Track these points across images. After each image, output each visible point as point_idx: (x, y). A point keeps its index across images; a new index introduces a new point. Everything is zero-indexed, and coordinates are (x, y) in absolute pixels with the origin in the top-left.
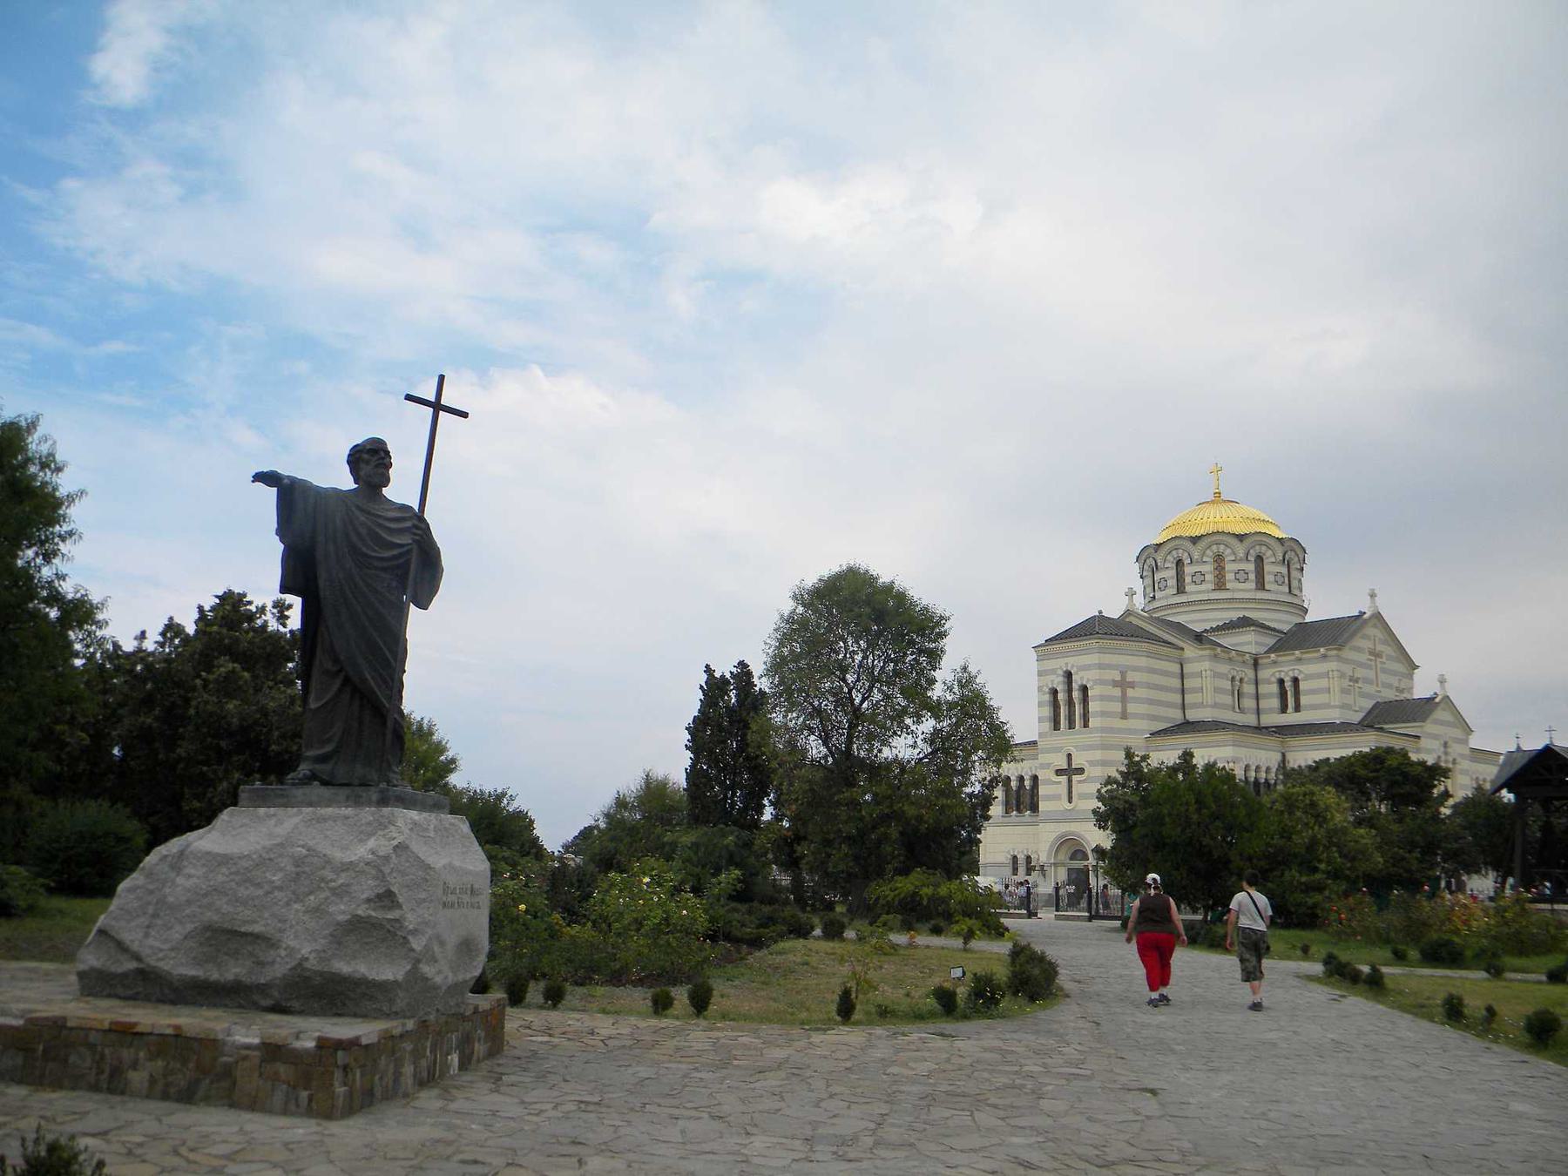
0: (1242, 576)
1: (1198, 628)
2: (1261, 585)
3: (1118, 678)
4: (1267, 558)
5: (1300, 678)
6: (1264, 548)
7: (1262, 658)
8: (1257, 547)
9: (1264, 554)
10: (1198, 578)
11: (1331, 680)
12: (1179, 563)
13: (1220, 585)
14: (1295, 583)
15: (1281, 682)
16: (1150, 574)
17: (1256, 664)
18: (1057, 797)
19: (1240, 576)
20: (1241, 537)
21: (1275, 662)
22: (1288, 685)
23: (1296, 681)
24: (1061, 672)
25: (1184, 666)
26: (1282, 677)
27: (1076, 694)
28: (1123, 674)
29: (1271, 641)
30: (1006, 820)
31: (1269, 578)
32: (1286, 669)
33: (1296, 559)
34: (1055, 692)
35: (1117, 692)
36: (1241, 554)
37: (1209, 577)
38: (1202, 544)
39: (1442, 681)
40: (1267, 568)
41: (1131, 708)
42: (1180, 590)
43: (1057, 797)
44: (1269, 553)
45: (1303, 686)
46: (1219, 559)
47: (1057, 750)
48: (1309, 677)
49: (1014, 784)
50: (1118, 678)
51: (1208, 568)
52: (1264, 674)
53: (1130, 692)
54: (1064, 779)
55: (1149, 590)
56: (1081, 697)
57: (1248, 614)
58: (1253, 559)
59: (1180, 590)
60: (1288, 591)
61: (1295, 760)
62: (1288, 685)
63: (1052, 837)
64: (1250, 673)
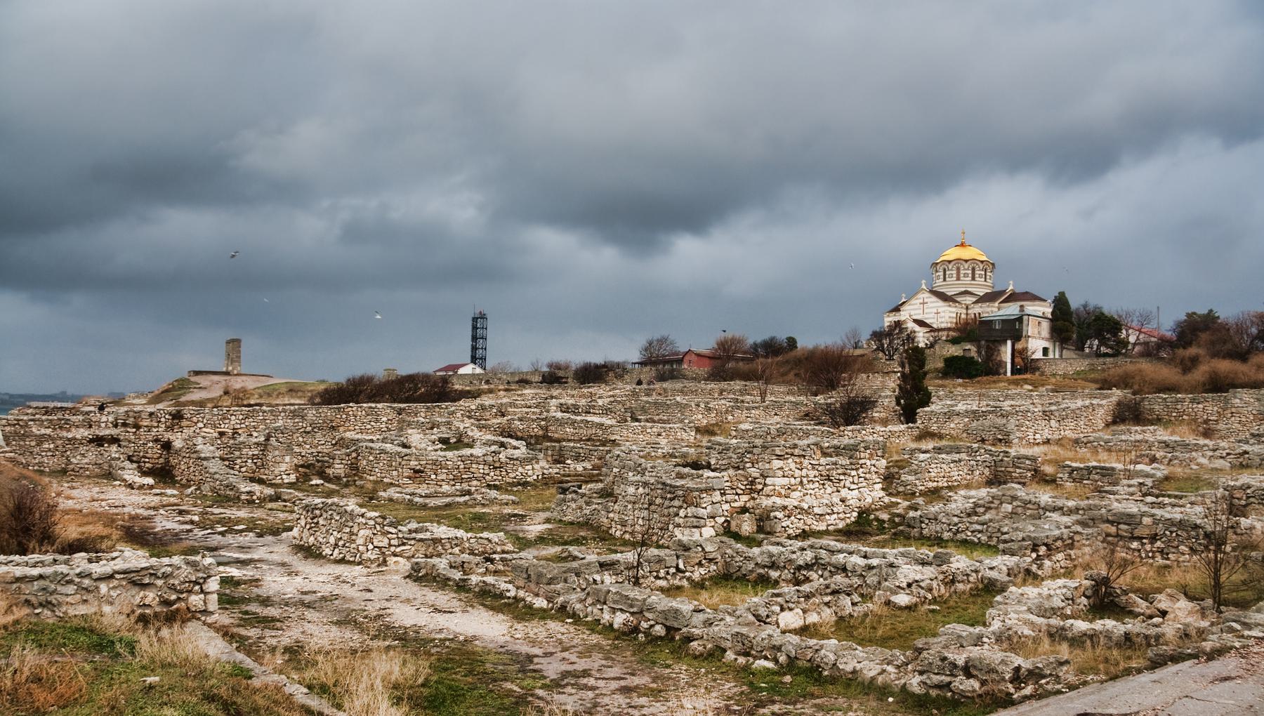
1: (949, 294)
2: (973, 279)
12: (945, 270)
13: (958, 279)
14: (988, 277)
17: (967, 308)
19: (966, 275)
20: (966, 261)
29: (974, 300)
36: (966, 267)
37: (955, 275)
38: (953, 263)
40: (977, 272)
42: (945, 280)
46: (958, 269)
51: (955, 272)
52: (969, 312)
57: (969, 289)
59: (945, 280)
60: (983, 279)
64: (965, 311)
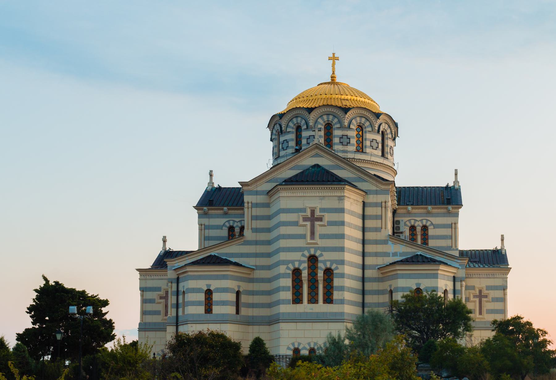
0: (375, 145)
6: (387, 126)
10: (345, 140)
11: (453, 229)
15: (413, 228)
16: (294, 130)
21: (409, 213)
22: (419, 229)
23: (425, 228)
26: (413, 224)
31: (387, 149)
32: (418, 219)
37: (353, 141)
39: (502, 240)
44: (389, 131)
45: (431, 232)
48: (436, 226)
51: (353, 134)
55: (292, 144)
62: (419, 229)
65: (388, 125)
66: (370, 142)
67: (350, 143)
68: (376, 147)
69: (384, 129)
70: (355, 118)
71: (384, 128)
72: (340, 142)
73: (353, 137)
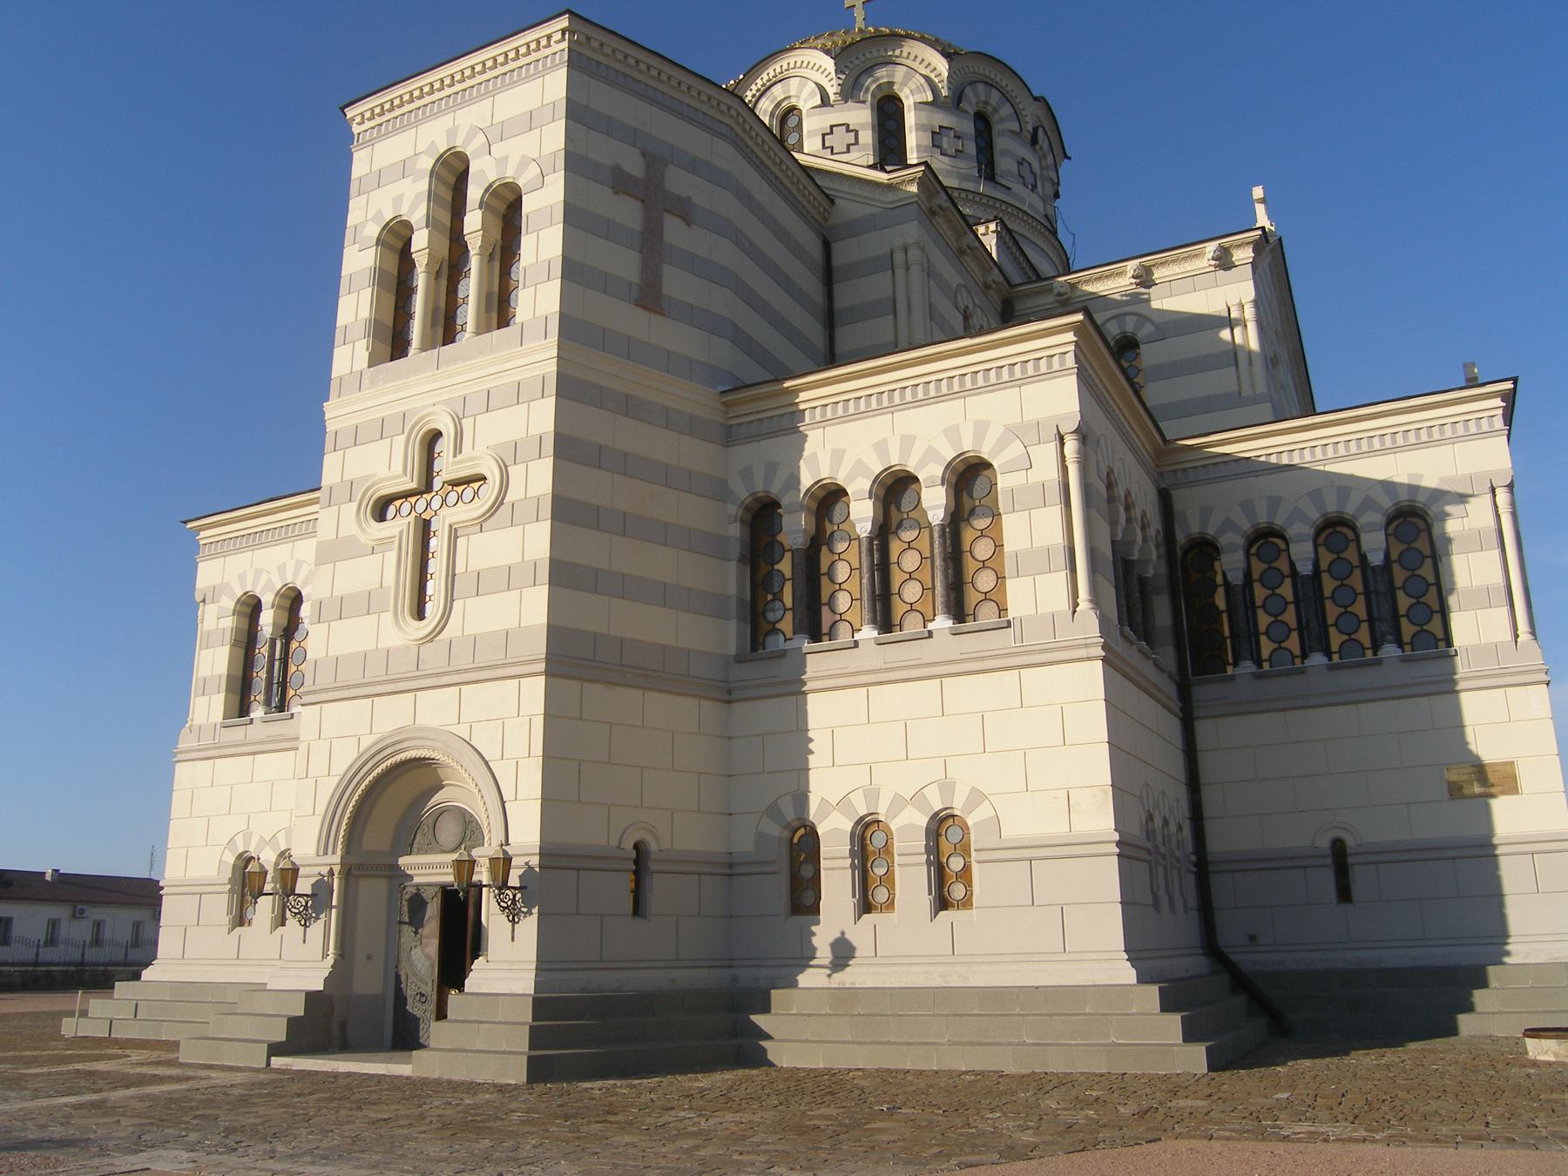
3: (634, 165)
4: (1002, 120)
5: (1140, 336)
6: (995, 97)
7: (1028, 295)
8: (981, 87)
9: (996, 110)
10: (840, 139)
18: (368, 604)
24: (427, 163)
25: (833, 246)
27: (473, 221)
28: (655, 161)
30: (237, 734)
31: (1004, 164)
33: (1050, 159)
34: (396, 238)
35: (628, 213)
36: (944, 92)
37: (867, 137)
40: (1002, 143)
41: (676, 284)
43: (368, 604)
44: (1006, 110)
45: (1150, 355)
47: (382, 430)
49: (267, 620)
50: (634, 165)
51: (861, 116)
53: (674, 230)
54: (400, 525)
56: (496, 235)
58: (972, 112)
61: (1206, 513)
63: (345, 757)
65: (1001, 93)
66: (930, 135)
67: (857, 143)
68: (957, 151)
69: (986, 103)
70: (869, 70)
71: (983, 99)
72: (824, 147)
73: (863, 126)
